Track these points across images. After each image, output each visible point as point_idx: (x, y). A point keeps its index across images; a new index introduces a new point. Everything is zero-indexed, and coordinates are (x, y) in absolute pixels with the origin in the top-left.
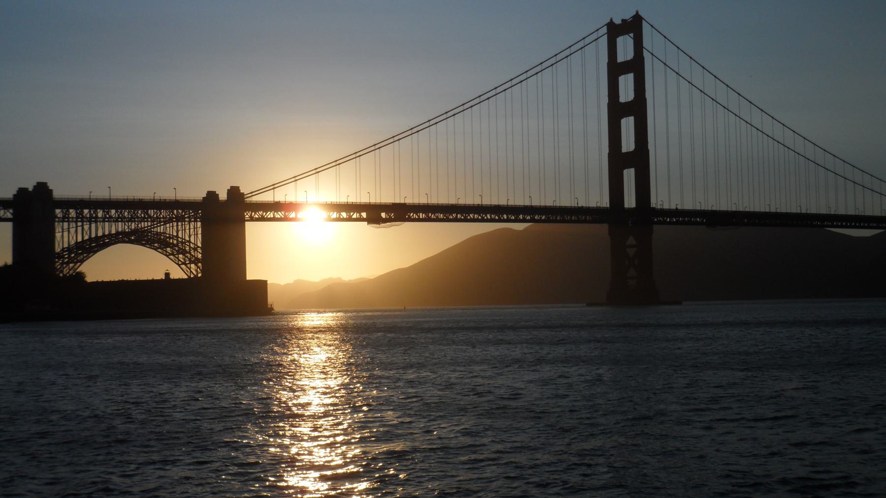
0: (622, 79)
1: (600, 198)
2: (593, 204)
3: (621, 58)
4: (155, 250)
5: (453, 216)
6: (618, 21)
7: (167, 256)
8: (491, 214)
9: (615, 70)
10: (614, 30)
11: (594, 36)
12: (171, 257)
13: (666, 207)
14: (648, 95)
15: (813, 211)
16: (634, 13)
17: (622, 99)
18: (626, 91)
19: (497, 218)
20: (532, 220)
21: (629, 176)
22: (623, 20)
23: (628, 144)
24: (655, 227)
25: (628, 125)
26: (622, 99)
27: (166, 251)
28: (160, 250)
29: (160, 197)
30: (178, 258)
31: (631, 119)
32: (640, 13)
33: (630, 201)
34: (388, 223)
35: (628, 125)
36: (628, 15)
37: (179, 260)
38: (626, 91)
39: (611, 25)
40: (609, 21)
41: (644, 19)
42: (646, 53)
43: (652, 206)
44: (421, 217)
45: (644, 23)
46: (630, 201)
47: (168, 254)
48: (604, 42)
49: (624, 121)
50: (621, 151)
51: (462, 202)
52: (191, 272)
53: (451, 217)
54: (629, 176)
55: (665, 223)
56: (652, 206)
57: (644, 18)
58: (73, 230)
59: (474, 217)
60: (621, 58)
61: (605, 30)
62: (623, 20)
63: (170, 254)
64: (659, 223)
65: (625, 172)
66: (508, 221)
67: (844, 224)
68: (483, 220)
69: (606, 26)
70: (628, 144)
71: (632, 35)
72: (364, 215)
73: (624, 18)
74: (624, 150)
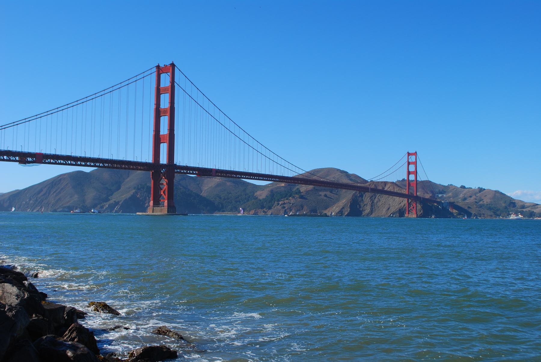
1: (149, 158)
2: (144, 161)
5: (48, 161)
6: (162, 65)
8: (71, 160)
9: (159, 92)
10: (160, 70)
11: (149, 72)
13: (182, 164)
15: (237, 170)
18: (165, 103)
19: (74, 163)
20: (99, 166)
21: (164, 148)
22: (164, 65)
23: (164, 130)
24: (176, 174)
25: (164, 121)
26: (162, 106)
32: (174, 63)
33: (164, 160)
34: (31, 164)
35: (164, 121)
36: (168, 63)
38: (165, 103)
39: (158, 67)
40: (158, 65)
42: (175, 84)
43: (174, 163)
44: (29, 160)
46: (164, 160)
48: (154, 76)
49: (162, 118)
51: (74, 154)
53: (47, 161)
54: (164, 148)
55: (180, 173)
56: (174, 163)
59: (61, 162)
60: (162, 85)
61: (155, 69)
64: (177, 172)
65: (162, 145)
66: (81, 165)
67: (247, 177)
68: (76, 165)
69: (155, 68)
70: (164, 130)
71: (169, 74)
72: (17, 158)
74: (161, 133)
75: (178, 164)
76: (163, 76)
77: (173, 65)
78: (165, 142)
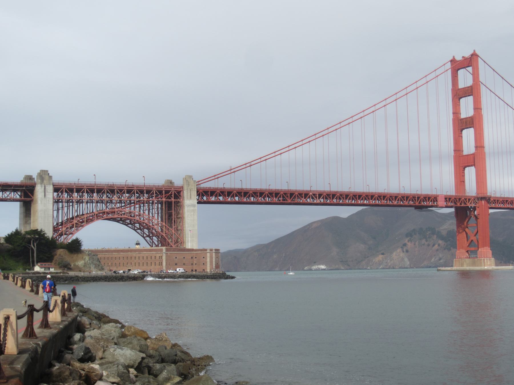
0: (462, 100)
3: (461, 85)
4: (127, 225)
6: (459, 58)
7: (135, 230)
11: (442, 70)
12: (139, 231)
14: (484, 112)
16: (472, 52)
17: (463, 116)
27: (135, 227)
28: (130, 225)
29: (133, 183)
30: (143, 231)
31: (472, 130)
36: (467, 55)
37: (144, 233)
40: (451, 58)
41: (479, 57)
43: (488, 194)
45: (479, 59)
47: (136, 228)
48: (450, 72)
50: (463, 154)
52: (153, 242)
54: (470, 173)
57: (479, 55)
58: (66, 209)
61: (449, 65)
62: (463, 57)
63: (138, 229)
69: (450, 62)
71: (470, 69)
73: (464, 56)
75: (492, 196)
76: (461, 72)
77: (474, 56)
78: (472, 166)
